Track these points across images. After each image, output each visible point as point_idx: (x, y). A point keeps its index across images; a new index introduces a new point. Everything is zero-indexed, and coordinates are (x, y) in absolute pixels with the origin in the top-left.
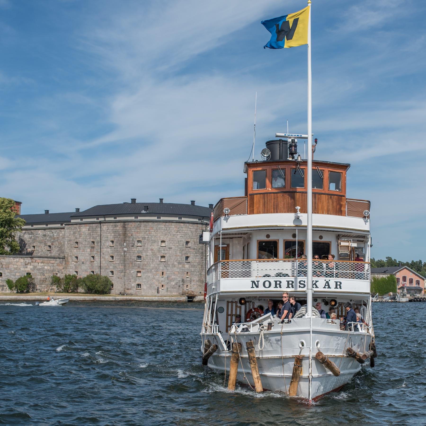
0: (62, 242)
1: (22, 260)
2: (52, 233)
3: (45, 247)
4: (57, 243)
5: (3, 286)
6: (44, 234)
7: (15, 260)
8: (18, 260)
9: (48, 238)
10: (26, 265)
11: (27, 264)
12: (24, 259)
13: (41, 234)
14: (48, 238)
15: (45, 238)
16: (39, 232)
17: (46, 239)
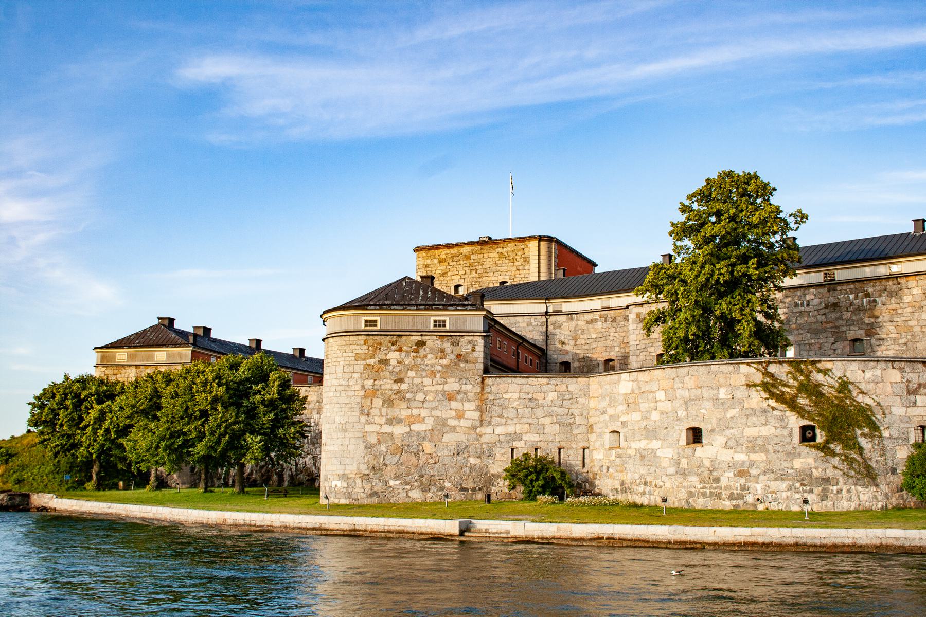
0: (911, 323)
1: (894, 375)
2: (867, 295)
3: (837, 345)
4: (892, 329)
5: (827, 480)
6: (832, 300)
7: (869, 375)
8: (878, 372)
9: (847, 315)
10: (910, 392)
11: (915, 392)
12: (902, 370)
13: (816, 301)
14: (847, 315)
15: (834, 315)
16: (808, 297)
17: (840, 318)
